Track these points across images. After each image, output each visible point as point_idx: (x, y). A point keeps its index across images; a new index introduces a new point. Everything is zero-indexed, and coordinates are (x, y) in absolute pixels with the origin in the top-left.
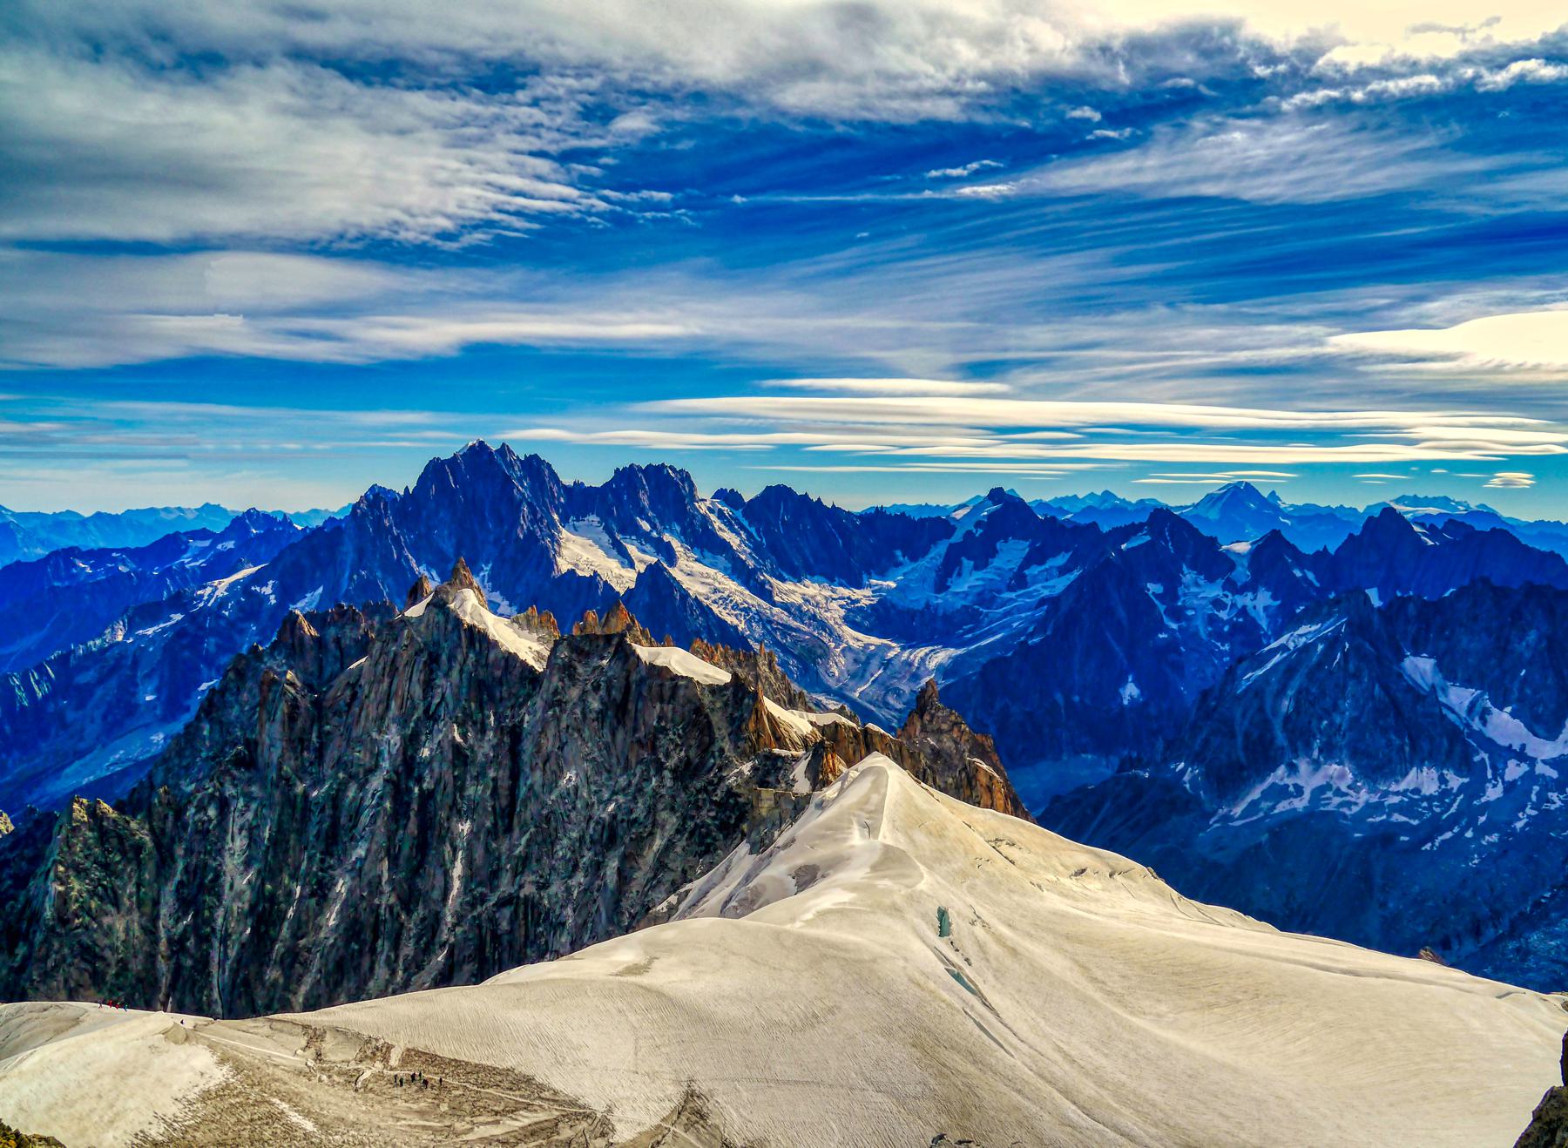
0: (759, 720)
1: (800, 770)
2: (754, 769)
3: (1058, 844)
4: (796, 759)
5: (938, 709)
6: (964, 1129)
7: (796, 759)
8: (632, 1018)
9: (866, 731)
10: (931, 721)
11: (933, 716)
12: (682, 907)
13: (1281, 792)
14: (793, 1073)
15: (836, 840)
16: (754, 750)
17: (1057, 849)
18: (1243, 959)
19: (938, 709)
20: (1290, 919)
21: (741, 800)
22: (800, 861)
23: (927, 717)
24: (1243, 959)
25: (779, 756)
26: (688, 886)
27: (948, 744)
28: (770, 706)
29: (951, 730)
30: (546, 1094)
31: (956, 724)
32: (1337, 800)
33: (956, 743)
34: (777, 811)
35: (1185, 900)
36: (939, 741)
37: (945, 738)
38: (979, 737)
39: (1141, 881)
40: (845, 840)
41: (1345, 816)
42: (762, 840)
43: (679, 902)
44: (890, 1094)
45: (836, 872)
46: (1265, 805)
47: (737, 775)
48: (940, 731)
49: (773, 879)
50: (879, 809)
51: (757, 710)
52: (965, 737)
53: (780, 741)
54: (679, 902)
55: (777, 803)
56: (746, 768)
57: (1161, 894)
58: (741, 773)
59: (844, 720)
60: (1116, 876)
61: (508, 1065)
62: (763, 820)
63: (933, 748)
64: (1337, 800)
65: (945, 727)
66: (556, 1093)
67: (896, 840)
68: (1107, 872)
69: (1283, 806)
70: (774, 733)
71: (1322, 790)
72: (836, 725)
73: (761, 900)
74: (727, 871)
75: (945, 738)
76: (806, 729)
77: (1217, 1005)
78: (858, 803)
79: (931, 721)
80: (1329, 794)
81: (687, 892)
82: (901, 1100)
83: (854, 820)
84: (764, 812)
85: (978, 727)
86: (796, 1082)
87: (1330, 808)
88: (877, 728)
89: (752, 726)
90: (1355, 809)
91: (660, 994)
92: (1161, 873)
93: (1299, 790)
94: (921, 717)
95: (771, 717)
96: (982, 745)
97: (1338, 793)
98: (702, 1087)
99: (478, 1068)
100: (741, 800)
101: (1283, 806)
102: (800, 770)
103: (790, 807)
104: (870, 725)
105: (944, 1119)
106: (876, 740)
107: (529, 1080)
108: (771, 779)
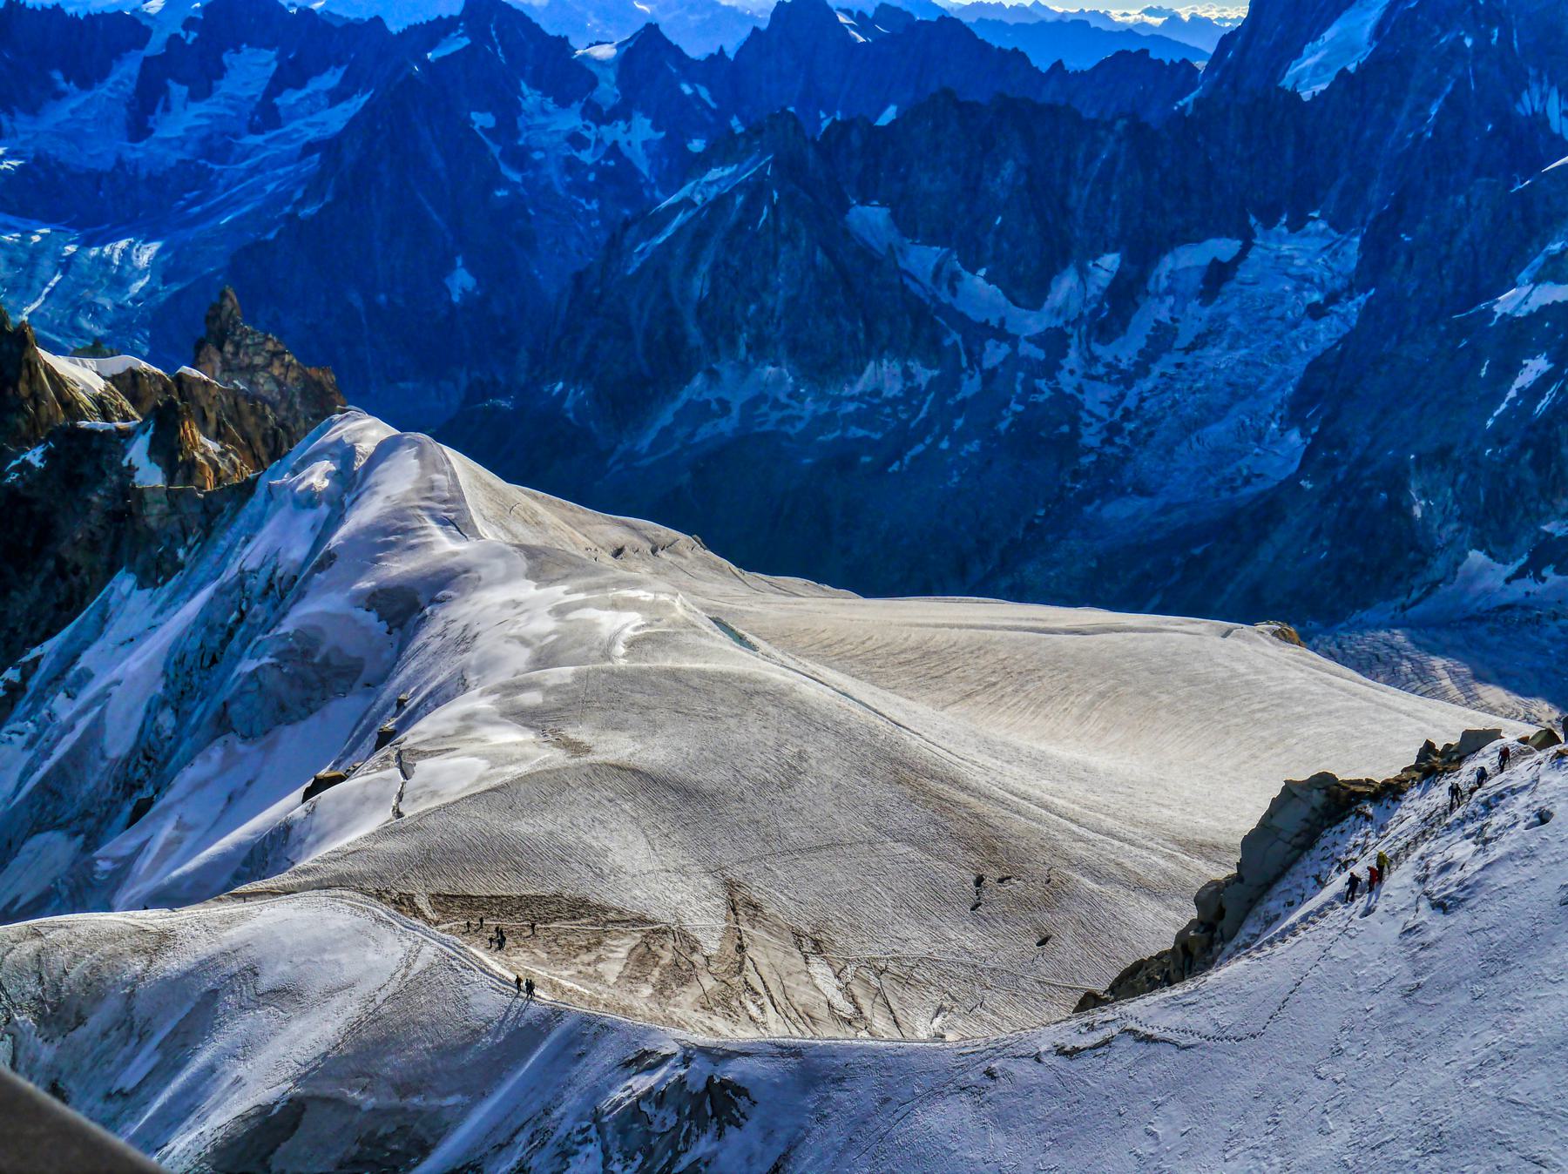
0: (33, 377)
1: (138, 452)
2: (47, 455)
3: (581, 516)
4: (128, 435)
5: (246, 334)
6: (997, 865)
7: (128, 435)
8: (626, 807)
9: (179, 379)
10: (236, 354)
11: (237, 345)
12: (33, 683)
13: (700, 411)
14: (810, 837)
15: (412, 547)
16: (34, 424)
17: (582, 524)
18: (964, 635)
19: (246, 334)
20: (869, 584)
21: (37, 508)
22: (365, 584)
23: (229, 348)
24: (964, 635)
25: (91, 433)
26: (35, 652)
27: (266, 386)
28: (46, 356)
29: (270, 364)
30: (612, 915)
31: (275, 354)
32: (776, 415)
33: (280, 384)
34: (175, 518)
35: (748, 576)
36: (251, 383)
37: (261, 378)
38: (315, 373)
39: (689, 554)
40: (427, 545)
41: (787, 436)
42: (158, 567)
43: (25, 677)
44: (910, 842)
45: (462, 591)
46: (681, 433)
47: (18, 469)
48: (252, 368)
49: (323, 614)
50: (457, 498)
51: (32, 365)
52: (293, 374)
53: (70, 405)
54: (25, 677)
55: (172, 505)
56: (35, 456)
57: (720, 569)
58: (26, 465)
59: (144, 365)
60: (659, 552)
61: (551, 889)
62: (152, 536)
63: (247, 396)
64: (776, 415)
65: (258, 360)
66: (620, 912)
67: (496, 535)
68: (647, 547)
69: (705, 431)
70: (60, 395)
71: (754, 402)
72: (134, 374)
73: (323, 650)
74: (104, 619)
75: (261, 378)
76: (99, 385)
77: (977, 693)
78: (418, 491)
79: (236, 354)
80: (764, 408)
81: (36, 662)
82: (921, 845)
83: (419, 512)
84: (152, 522)
85: (306, 358)
86: (819, 848)
87: (766, 428)
88: (196, 373)
89: (23, 388)
90: (800, 426)
91: (635, 771)
92: (711, 543)
93: (725, 406)
94: (220, 349)
95: (51, 373)
96: (319, 384)
97: (776, 404)
98: (737, 873)
99: (525, 902)
100: (37, 508)
101: (705, 431)
102: (138, 452)
103: (197, 509)
104: (185, 369)
105: (973, 858)
106: (199, 391)
107: (584, 903)
108: (86, 469)
